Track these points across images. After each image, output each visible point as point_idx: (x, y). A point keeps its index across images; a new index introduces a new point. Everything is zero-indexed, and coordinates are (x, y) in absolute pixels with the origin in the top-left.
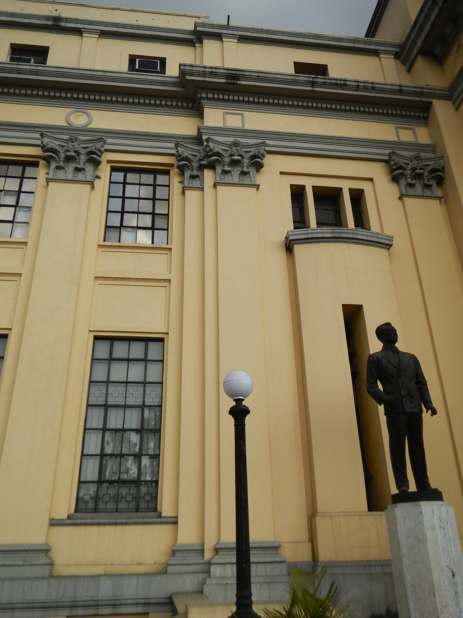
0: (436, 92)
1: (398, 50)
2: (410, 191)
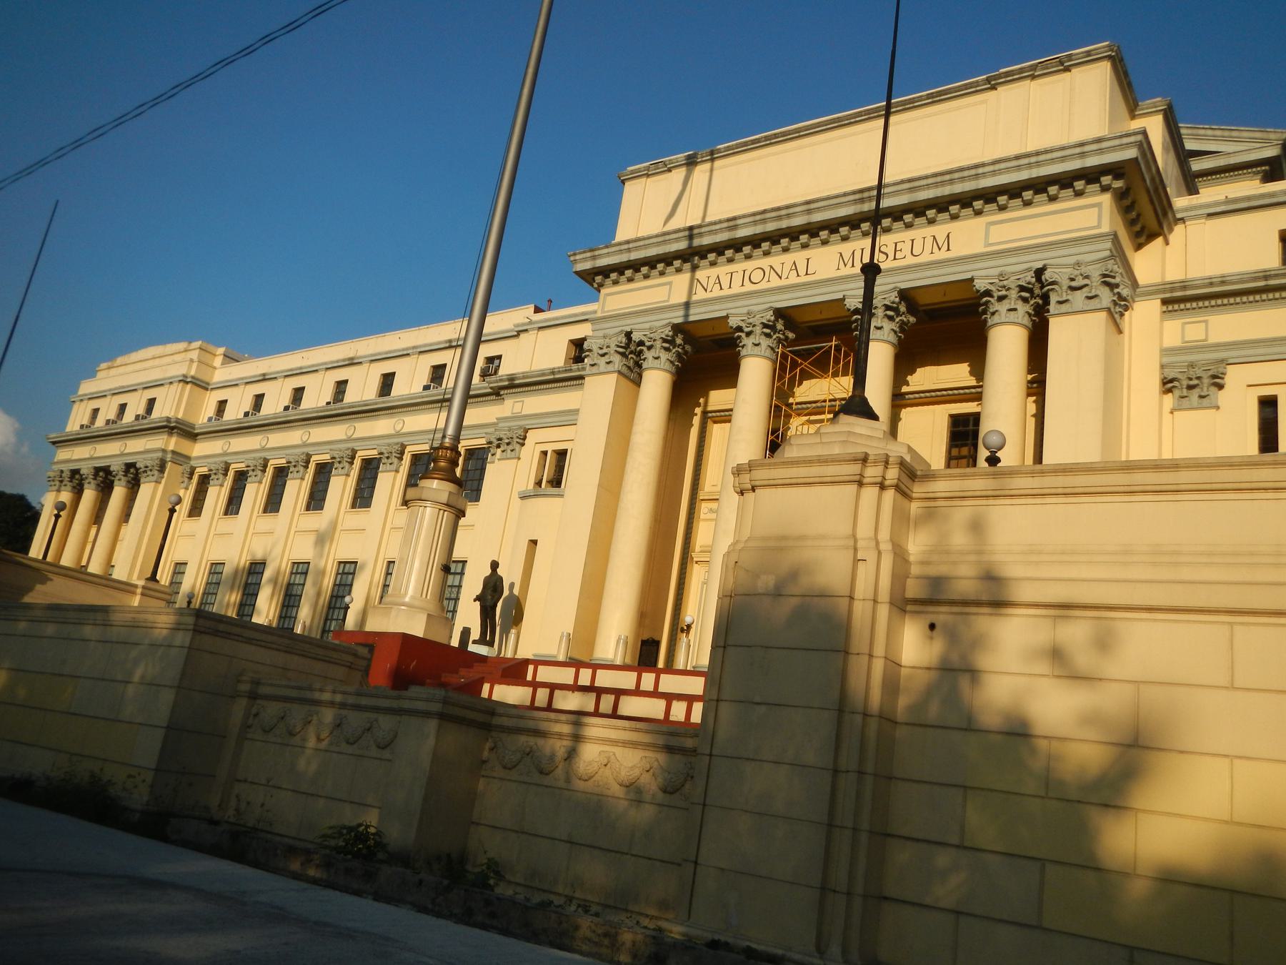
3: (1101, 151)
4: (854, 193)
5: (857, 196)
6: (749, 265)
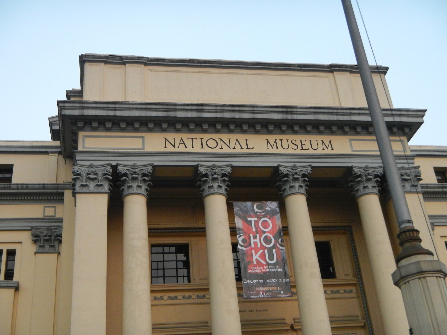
0: (67, 186)
1: (60, 150)
2: (41, 250)
3: (408, 116)
4: (282, 107)
5: (284, 110)
6: (206, 136)
